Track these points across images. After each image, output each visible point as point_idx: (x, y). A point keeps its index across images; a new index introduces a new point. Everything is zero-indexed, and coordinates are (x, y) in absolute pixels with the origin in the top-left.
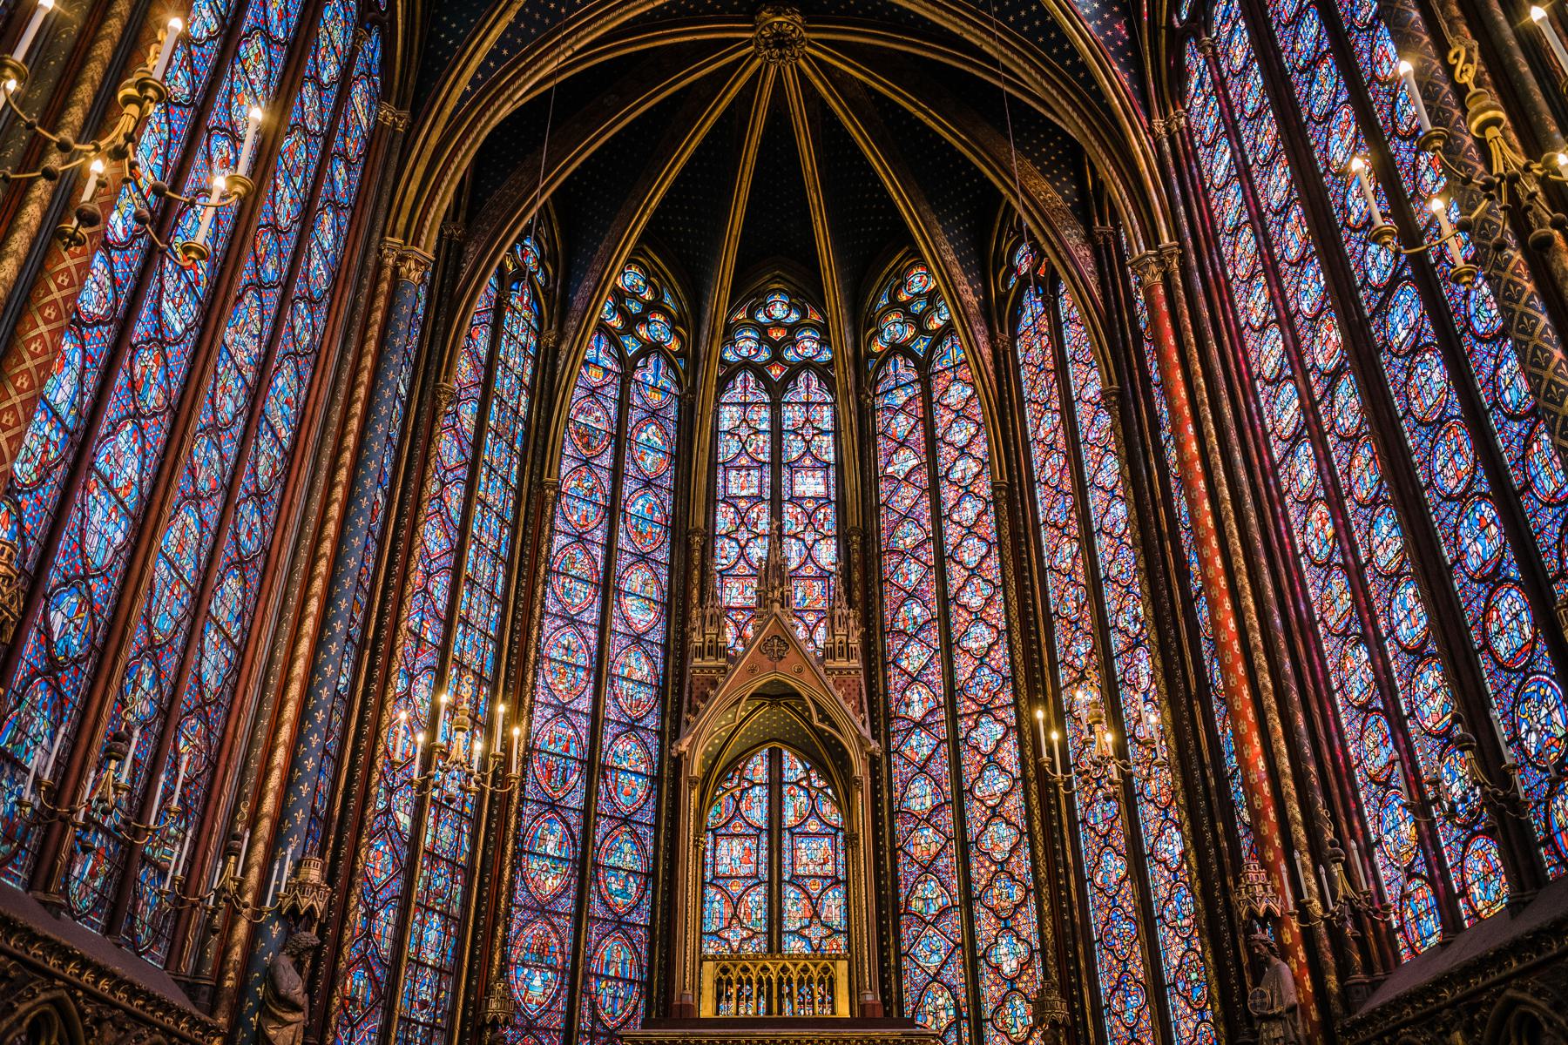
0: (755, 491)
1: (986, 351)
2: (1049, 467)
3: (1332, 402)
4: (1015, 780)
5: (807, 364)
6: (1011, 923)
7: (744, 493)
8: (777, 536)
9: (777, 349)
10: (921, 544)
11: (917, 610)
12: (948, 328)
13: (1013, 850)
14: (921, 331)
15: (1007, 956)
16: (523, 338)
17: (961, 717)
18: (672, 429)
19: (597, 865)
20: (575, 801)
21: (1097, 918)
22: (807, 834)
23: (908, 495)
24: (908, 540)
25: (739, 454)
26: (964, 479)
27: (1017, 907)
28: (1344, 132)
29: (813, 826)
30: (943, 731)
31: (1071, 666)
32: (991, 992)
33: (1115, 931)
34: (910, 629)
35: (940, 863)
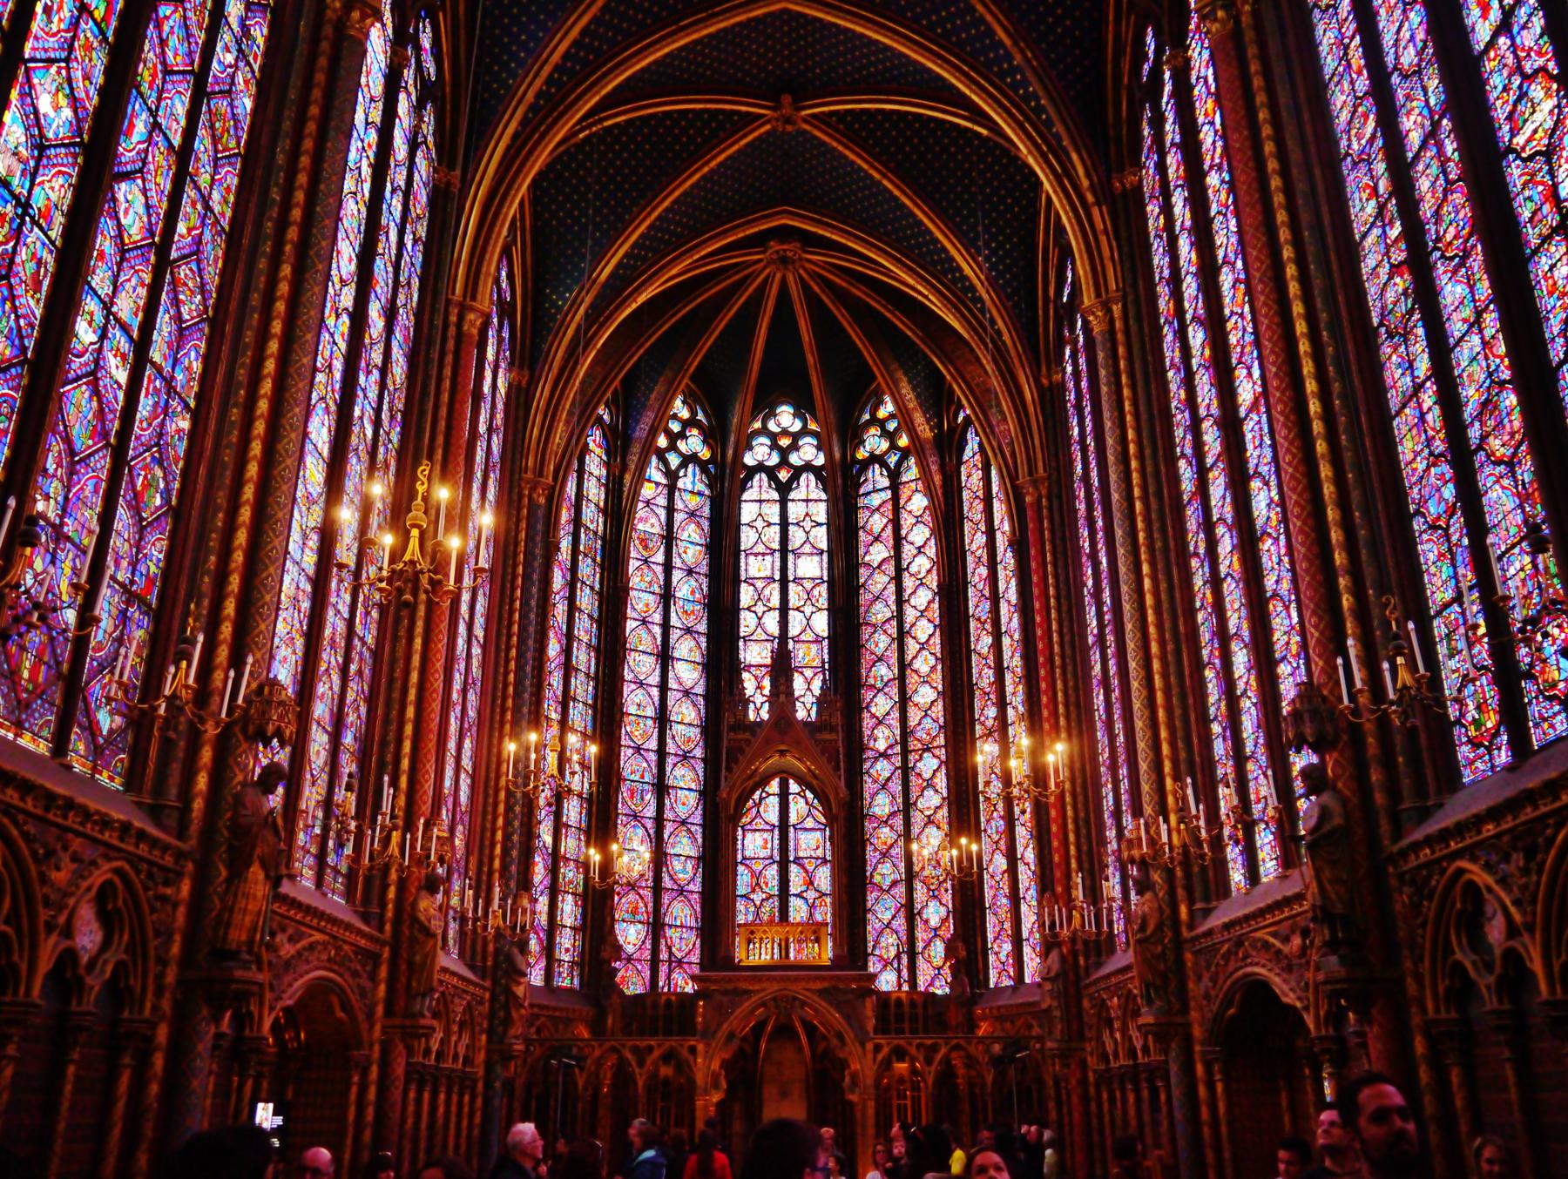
0: (768, 573)
1: (937, 479)
2: (977, 574)
5: (808, 467)
8: (784, 609)
9: (784, 453)
10: (889, 620)
14: (893, 446)
15: (934, 913)
16: (596, 472)
18: (706, 525)
19: (666, 854)
20: (650, 812)
21: (988, 894)
22: (805, 829)
29: (810, 823)
30: (898, 762)
31: (983, 724)
32: (921, 935)
34: (879, 685)
35: (893, 852)
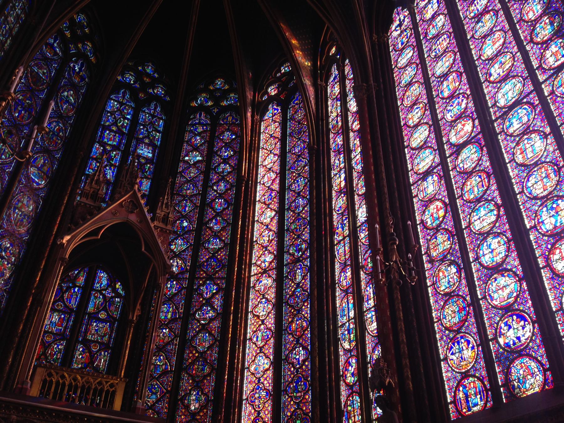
3: (457, 158)
4: (218, 314)
6: (200, 384)
7: (110, 143)
9: (144, 87)
11: (185, 224)
12: (229, 108)
13: (210, 347)
17: (197, 278)
21: (247, 388)
23: (193, 173)
24: (188, 192)
25: (113, 124)
26: (223, 172)
27: (205, 377)
29: (102, 315)
33: (257, 395)
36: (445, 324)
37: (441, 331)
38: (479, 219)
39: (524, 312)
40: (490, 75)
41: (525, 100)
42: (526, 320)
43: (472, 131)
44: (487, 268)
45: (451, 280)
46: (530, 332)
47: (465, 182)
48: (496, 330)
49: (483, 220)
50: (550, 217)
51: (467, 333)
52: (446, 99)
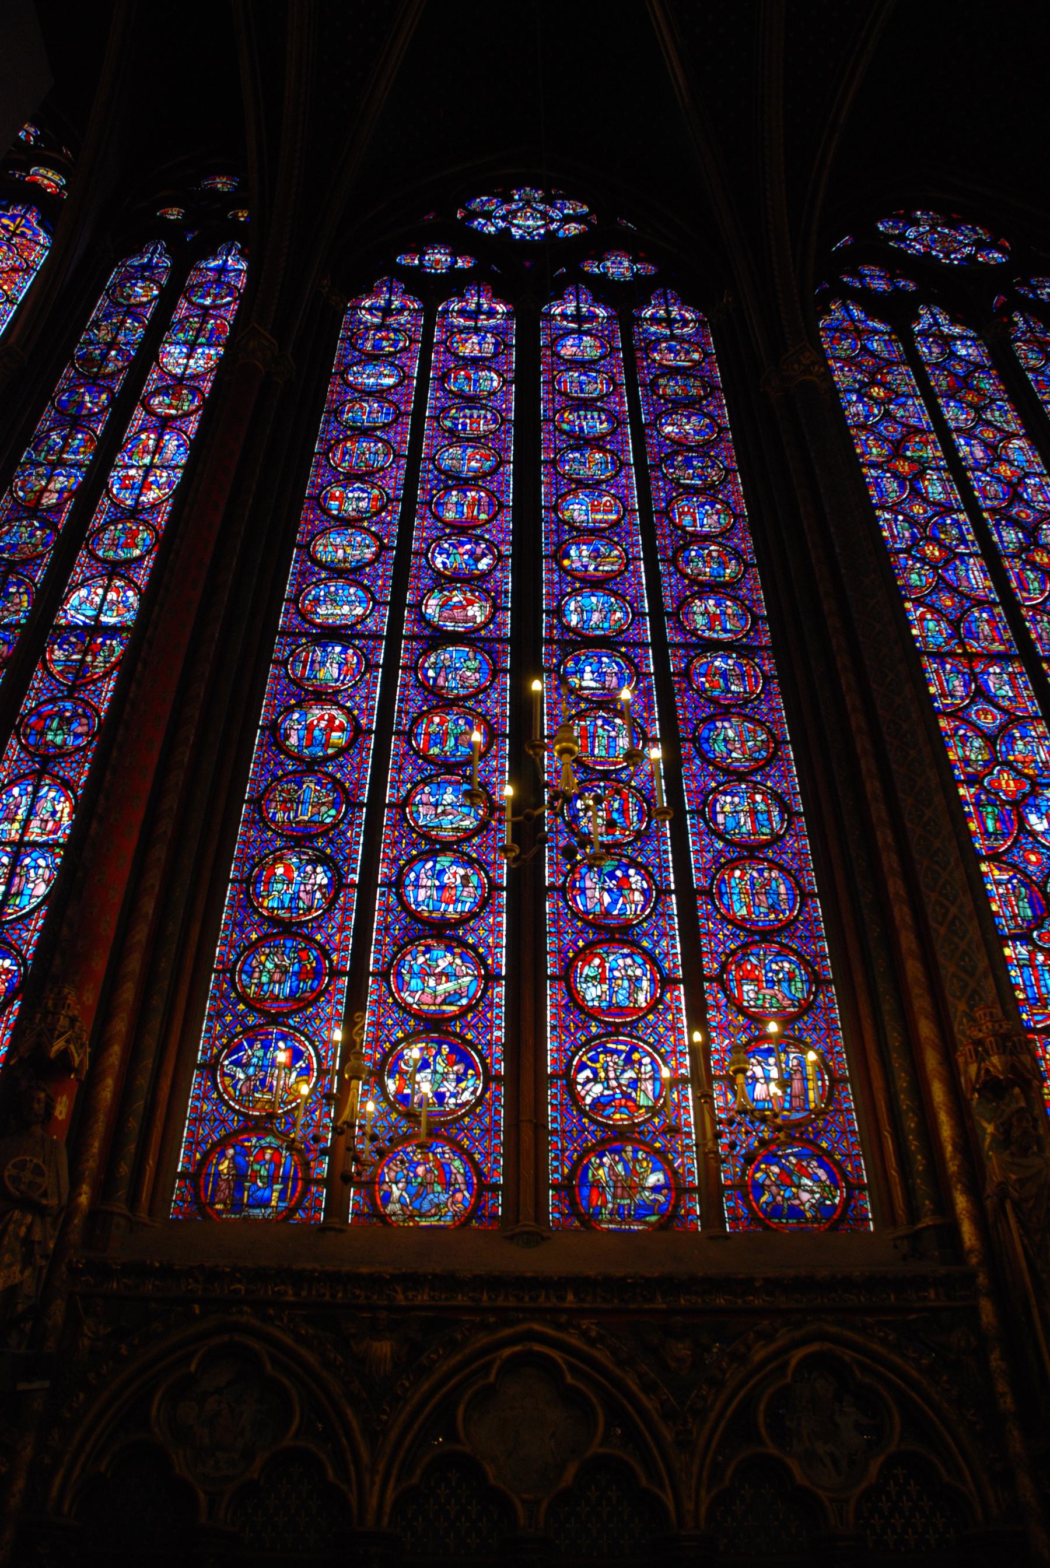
3: (426, 654)
28: (596, 511)
36: (244, 987)
37: (225, 996)
38: (436, 806)
39: (474, 1047)
40: (567, 556)
41: (623, 650)
42: (470, 1064)
43: (485, 625)
44: (415, 916)
45: (302, 895)
46: (473, 1093)
47: (428, 712)
48: (386, 1055)
49: (444, 813)
50: (603, 889)
51: (302, 1033)
52: (447, 524)
